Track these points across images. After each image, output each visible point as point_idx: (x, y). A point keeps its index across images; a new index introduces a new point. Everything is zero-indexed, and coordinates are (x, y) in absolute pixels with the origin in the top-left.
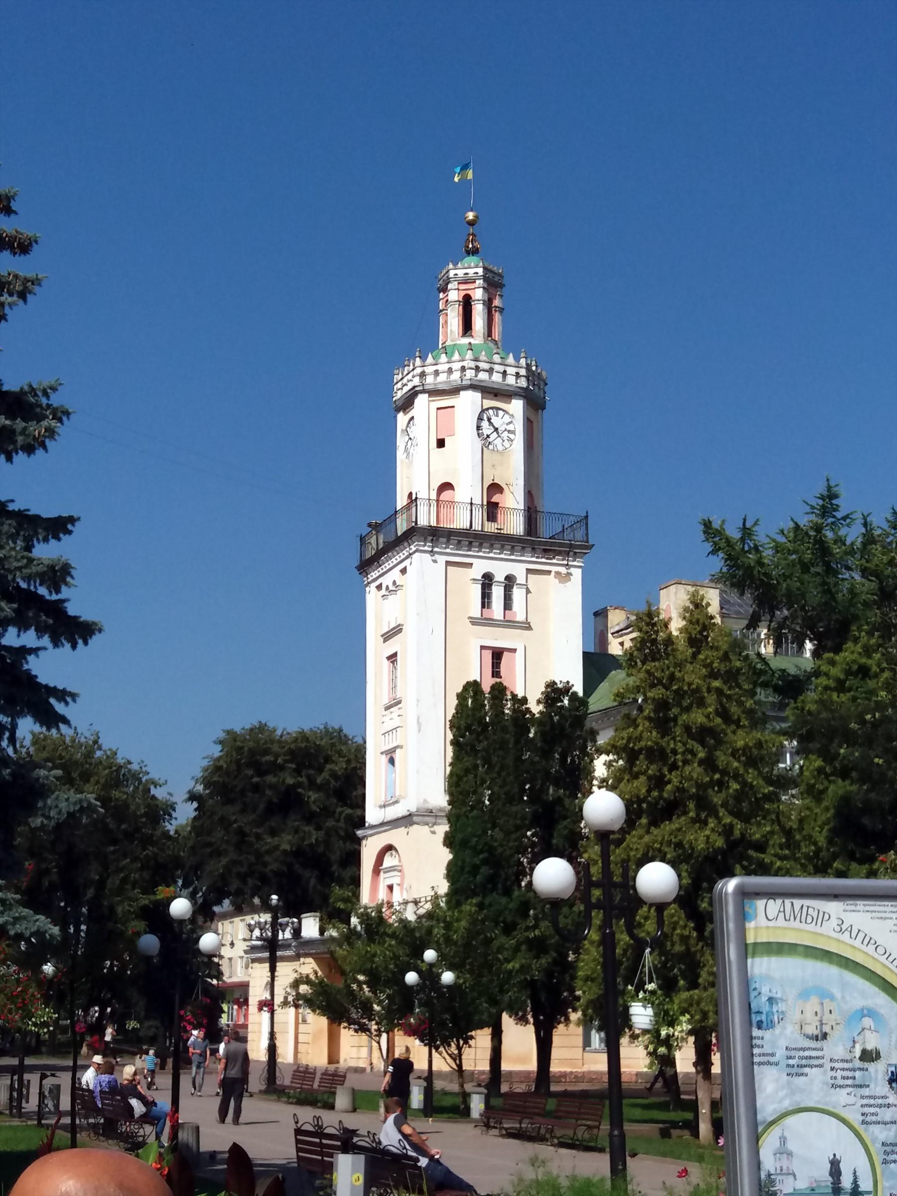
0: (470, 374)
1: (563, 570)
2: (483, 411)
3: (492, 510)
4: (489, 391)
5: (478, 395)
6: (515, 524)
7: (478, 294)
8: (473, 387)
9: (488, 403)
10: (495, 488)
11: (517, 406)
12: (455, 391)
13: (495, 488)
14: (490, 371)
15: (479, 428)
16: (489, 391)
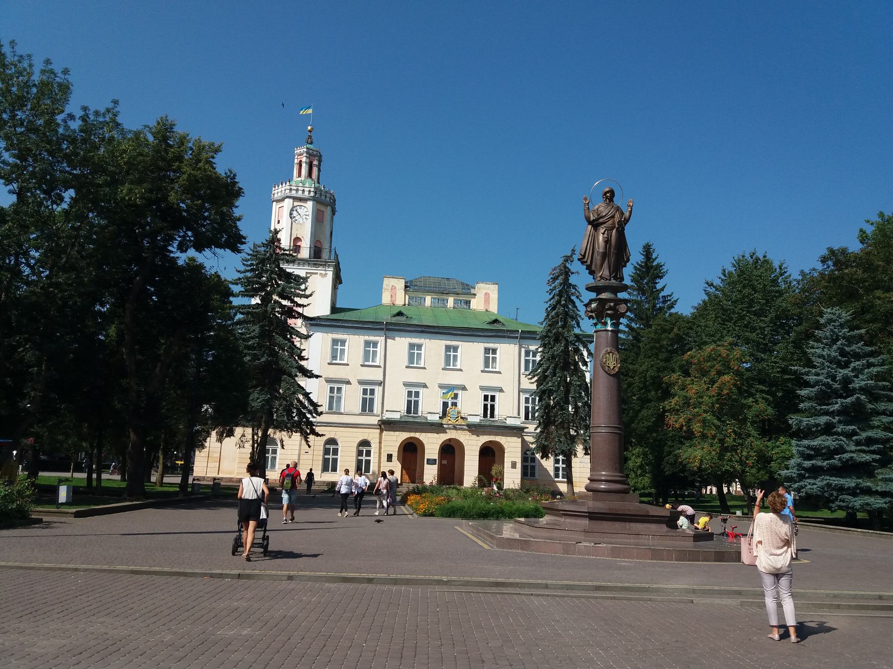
0: (294, 192)
1: (323, 272)
2: (294, 207)
3: (297, 248)
4: (295, 199)
5: (292, 200)
6: (305, 253)
7: (304, 159)
8: (288, 197)
9: (296, 204)
10: (297, 239)
11: (310, 204)
12: (283, 200)
13: (297, 239)
14: (297, 190)
15: (291, 214)
16: (295, 199)
